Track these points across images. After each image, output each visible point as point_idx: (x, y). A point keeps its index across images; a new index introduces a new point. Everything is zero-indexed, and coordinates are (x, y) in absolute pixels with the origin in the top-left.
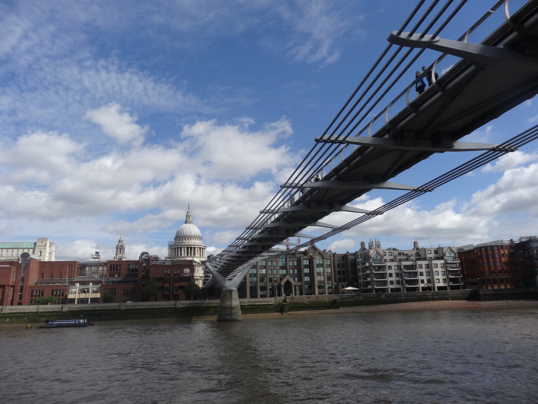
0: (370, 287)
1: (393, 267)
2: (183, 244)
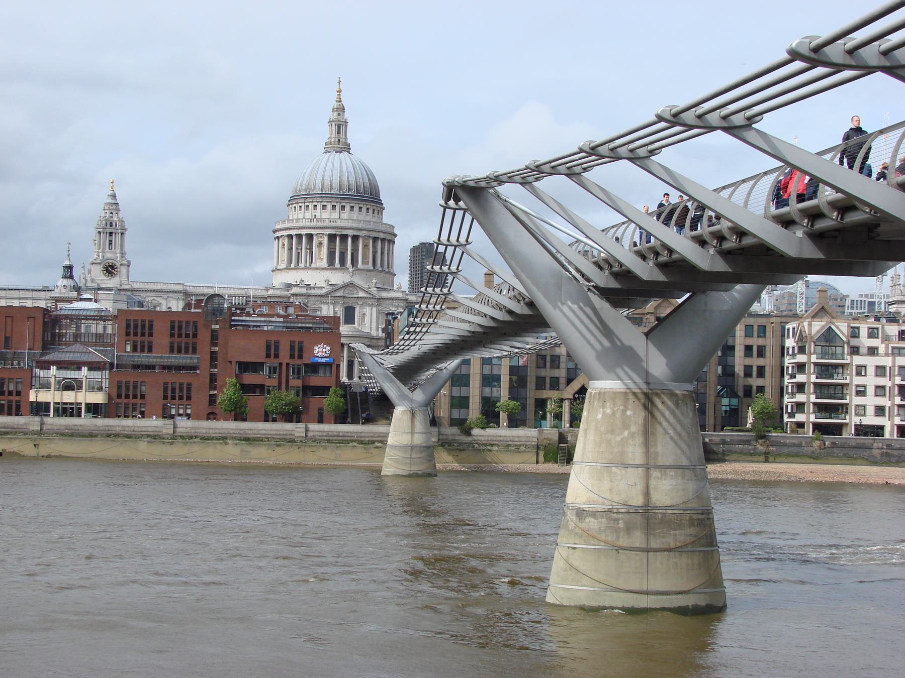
1: (871, 371)
2: (314, 224)
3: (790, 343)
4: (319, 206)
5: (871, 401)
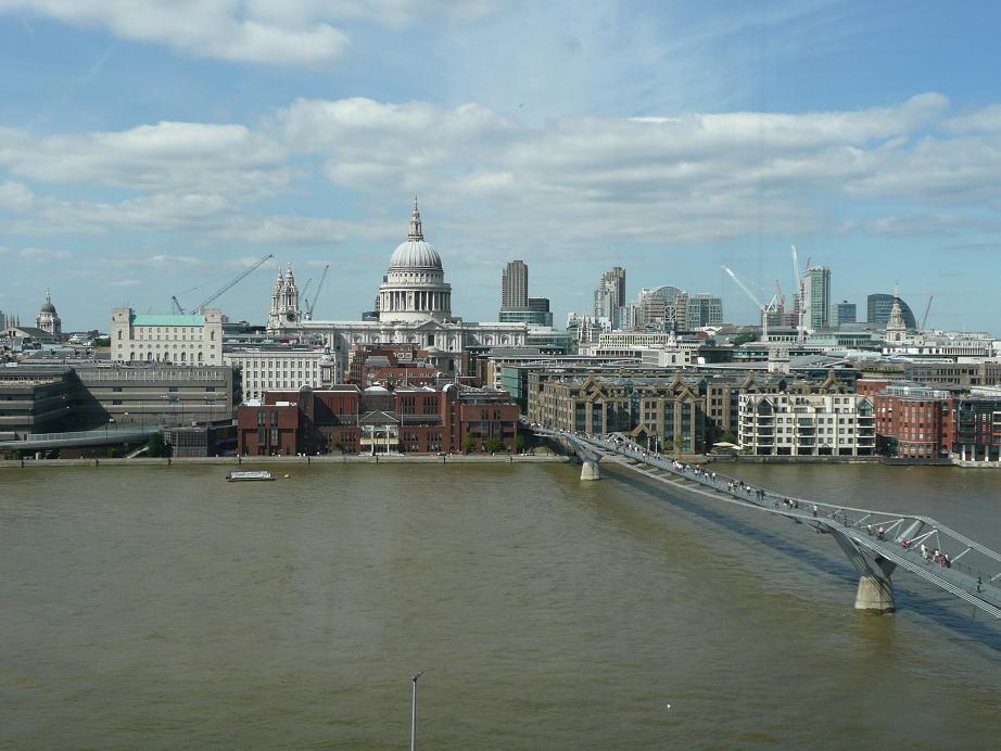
0: (750, 444)
1: (785, 420)
2: (406, 285)
3: (742, 404)
4: (409, 274)
5: (784, 435)
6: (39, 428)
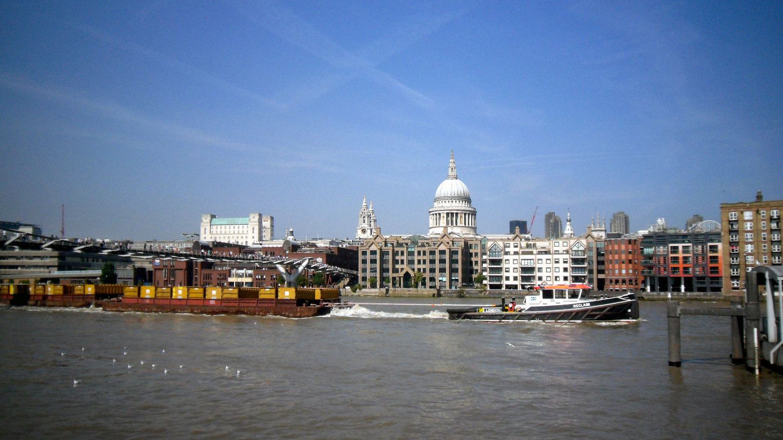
4: (444, 201)
6: (61, 267)
